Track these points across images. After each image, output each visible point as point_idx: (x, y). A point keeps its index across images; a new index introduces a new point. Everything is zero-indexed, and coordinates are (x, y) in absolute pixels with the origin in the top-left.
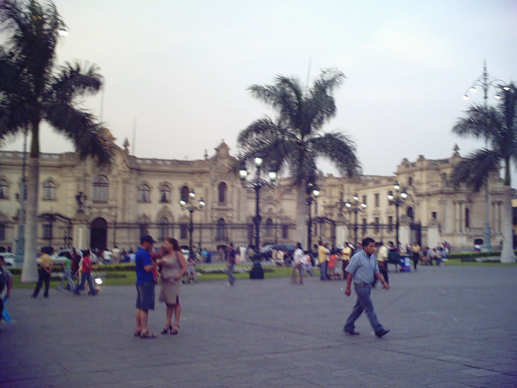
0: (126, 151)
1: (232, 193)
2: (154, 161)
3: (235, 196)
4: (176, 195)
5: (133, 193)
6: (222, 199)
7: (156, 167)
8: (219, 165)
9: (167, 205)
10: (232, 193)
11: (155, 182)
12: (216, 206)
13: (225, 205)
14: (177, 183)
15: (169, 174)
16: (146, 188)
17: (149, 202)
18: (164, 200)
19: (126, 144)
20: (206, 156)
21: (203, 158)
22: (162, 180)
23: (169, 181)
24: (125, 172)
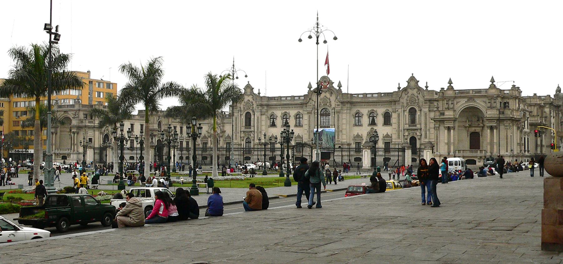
0: (340, 90)
1: (420, 115)
2: (365, 95)
3: (423, 118)
4: (380, 120)
5: (265, 121)
6: (413, 121)
7: (366, 100)
8: (409, 95)
9: (375, 128)
10: (420, 115)
11: (365, 111)
12: (407, 127)
13: (250, 128)
14: (380, 111)
15: (375, 104)
16: (358, 115)
17: (361, 125)
18: (373, 123)
19: (340, 86)
20: (399, 88)
21: (397, 90)
22: (370, 109)
23: (375, 109)
24: (338, 105)
